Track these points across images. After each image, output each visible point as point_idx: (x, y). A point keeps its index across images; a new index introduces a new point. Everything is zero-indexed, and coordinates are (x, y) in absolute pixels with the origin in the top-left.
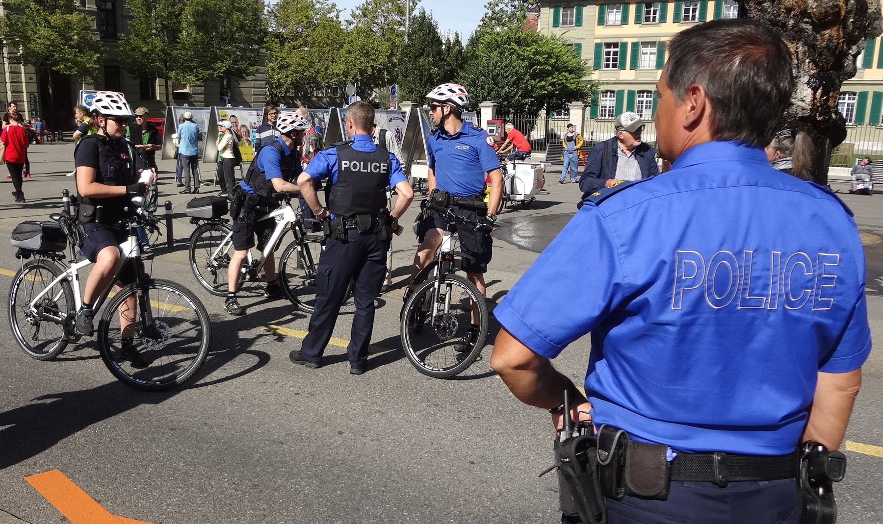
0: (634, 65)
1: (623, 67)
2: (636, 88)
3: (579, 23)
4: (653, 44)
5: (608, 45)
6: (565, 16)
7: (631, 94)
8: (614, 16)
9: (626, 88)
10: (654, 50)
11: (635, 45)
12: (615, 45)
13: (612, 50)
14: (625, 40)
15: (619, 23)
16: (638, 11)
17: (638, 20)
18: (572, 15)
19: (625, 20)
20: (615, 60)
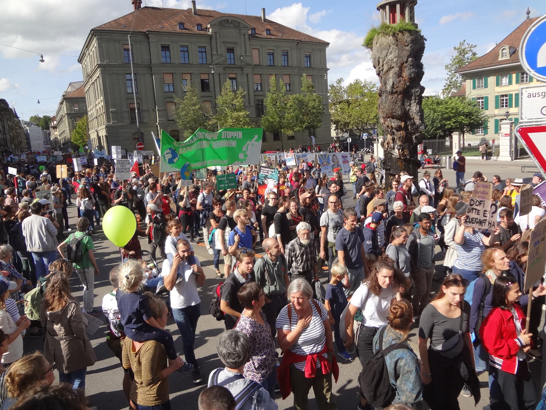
1: (511, 106)
3: (486, 86)
5: (503, 96)
6: (479, 83)
8: (505, 80)
12: (506, 96)
13: (505, 98)
14: (511, 93)
15: (507, 84)
16: (517, 77)
17: (517, 82)
18: (482, 82)
19: (510, 83)
20: (506, 103)
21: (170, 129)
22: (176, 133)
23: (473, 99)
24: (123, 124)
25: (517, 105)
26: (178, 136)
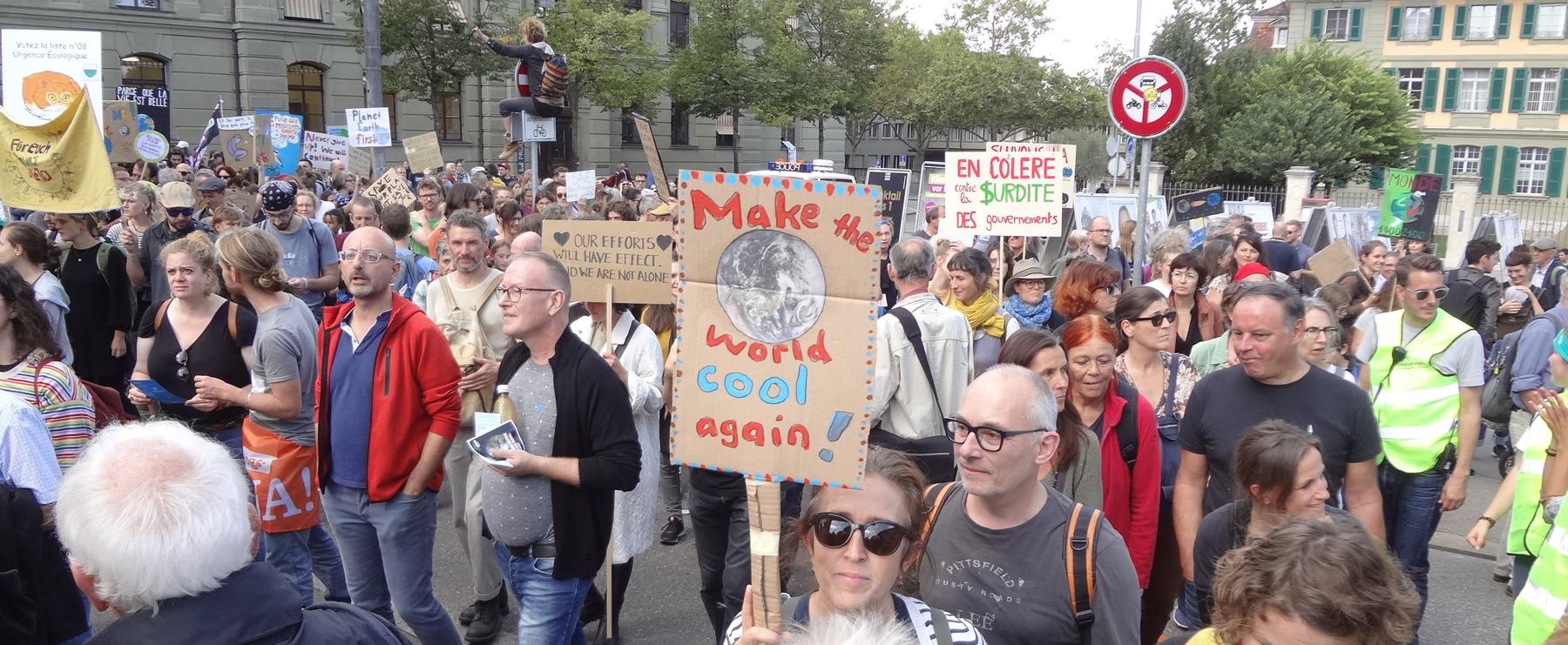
0: (1450, 105)
1: (1430, 106)
2: (1519, 144)
4: (1550, 72)
5: (1405, 72)
7: (1510, 153)
9: (1500, 144)
10: (1487, 79)
11: (1519, 73)
12: (1418, 73)
13: (1411, 80)
14: (1434, 65)
15: (1491, 35)
18: (1343, 23)
21: (293, 52)
22: (311, 77)
23: (1390, 72)
24: (80, 7)
25: (1450, 105)
26: (320, 89)
